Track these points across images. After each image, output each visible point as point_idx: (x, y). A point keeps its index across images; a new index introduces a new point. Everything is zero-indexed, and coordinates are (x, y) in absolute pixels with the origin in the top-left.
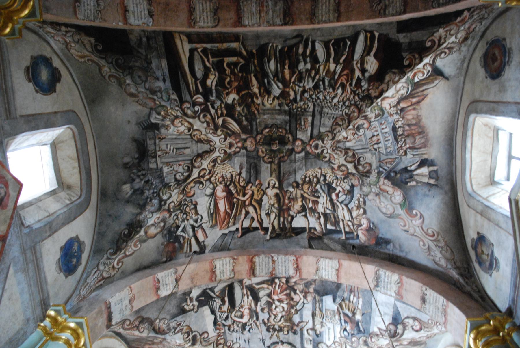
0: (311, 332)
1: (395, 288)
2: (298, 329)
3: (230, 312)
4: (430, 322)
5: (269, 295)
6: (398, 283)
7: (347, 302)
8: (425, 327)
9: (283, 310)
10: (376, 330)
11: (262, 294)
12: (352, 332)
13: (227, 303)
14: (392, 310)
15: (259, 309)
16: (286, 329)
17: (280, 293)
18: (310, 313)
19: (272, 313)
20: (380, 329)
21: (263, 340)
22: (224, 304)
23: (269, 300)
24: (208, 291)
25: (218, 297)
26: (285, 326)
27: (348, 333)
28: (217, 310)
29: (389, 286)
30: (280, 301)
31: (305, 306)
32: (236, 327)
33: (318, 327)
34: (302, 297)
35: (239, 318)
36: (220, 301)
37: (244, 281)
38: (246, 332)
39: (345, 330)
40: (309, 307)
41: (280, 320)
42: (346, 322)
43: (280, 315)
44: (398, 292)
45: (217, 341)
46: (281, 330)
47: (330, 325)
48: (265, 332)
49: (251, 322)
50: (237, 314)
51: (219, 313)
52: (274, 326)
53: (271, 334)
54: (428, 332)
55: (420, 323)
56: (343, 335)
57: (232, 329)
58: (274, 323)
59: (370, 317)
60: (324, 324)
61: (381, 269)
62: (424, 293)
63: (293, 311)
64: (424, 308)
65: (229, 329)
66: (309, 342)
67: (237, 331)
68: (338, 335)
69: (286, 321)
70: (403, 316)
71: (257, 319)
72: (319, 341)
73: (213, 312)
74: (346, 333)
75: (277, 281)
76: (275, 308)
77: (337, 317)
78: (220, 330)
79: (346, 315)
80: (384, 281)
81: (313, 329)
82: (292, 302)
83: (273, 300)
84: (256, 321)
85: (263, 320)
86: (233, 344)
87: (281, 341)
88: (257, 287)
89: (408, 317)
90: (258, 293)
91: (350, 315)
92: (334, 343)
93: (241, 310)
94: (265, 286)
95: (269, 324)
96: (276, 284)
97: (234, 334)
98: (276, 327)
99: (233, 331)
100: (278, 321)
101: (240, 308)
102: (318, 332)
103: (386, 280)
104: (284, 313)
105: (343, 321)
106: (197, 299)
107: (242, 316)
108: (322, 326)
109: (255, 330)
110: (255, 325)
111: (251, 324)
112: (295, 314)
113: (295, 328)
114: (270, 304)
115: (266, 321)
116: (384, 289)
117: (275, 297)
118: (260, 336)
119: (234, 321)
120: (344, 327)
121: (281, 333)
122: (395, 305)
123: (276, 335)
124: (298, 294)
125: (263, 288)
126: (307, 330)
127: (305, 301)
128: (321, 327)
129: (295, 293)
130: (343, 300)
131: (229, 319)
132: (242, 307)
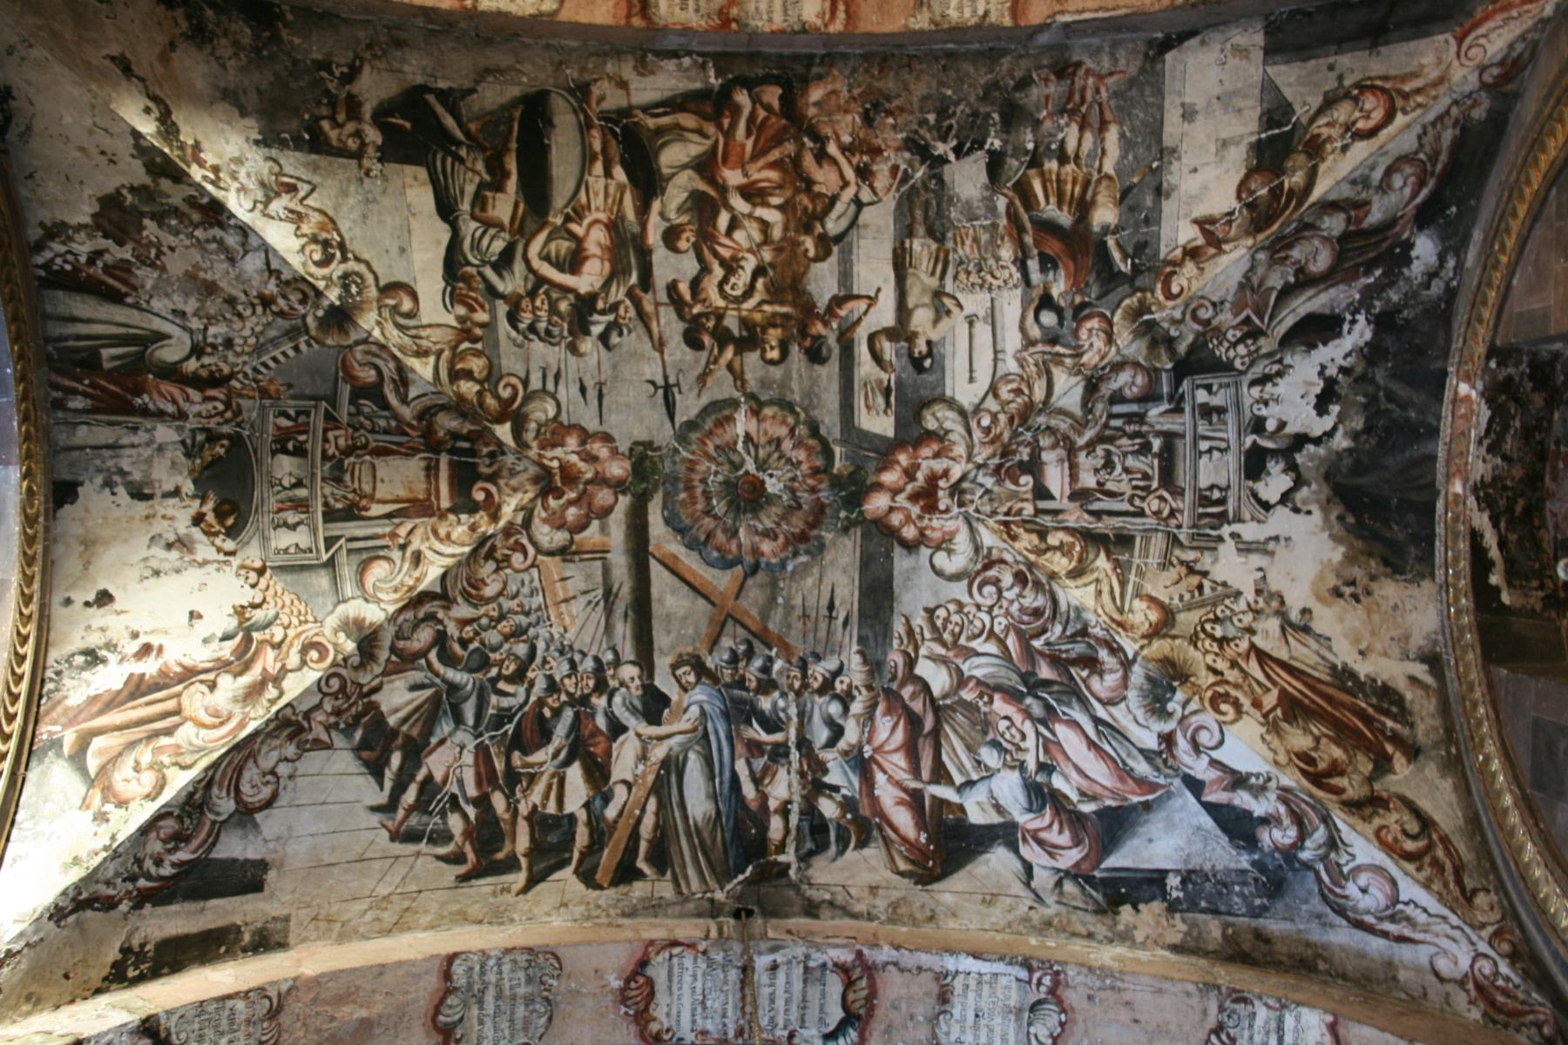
0: (888, 349)
2: (832, 340)
3: (521, 231)
5: (705, 166)
7: (1052, 165)
9: (767, 240)
11: (672, 156)
12: (1078, 299)
13: (512, 184)
15: (654, 237)
16: (774, 335)
17: (755, 157)
18: (886, 250)
19: (716, 254)
21: (667, 388)
22: (498, 187)
23: (702, 186)
24: (431, 98)
25: (474, 142)
26: (771, 322)
27: (1059, 312)
28: (465, 206)
30: (752, 193)
31: (867, 215)
32: (543, 314)
33: (921, 319)
34: (850, 174)
35: (560, 267)
36: (480, 166)
37: (596, 91)
38: (587, 345)
39: (1046, 302)
40: (880, 218)
41: (750, 291)
42: (1047, 263)
43: (750, 264)
45: (456, 356)
46: (750, 339)
47: (975, 303)
48: (677, 350)
49: (618, 293)
50: (553, 246)
51: (474, 225)
52: (720, 317)
53: (704, 355)
56: (1035, 332)
57: (527, 318)
58: (721, 303)
60: (948, 302)
63: (809, 244)
65: (513, 319)
66: (880, 401)
67: (548, 332)
68: (1012, 341)
69: (775, 294)
71: (646, 282)
72: (925, 393)
73: (446, 209)
74: (1048, 318)
75: (742, 98)
76: (729, 232)
77: (1007, 253)
78: (472, 309)
79: (1047, 228)
81: (900, 331)
82: (805, 200)
83: (723, 189)
84: (638, 292)
85: (672, 287)
86: (529, 398)
87: (752, 397)
88: (651, 123)
90: (657, 154)
91: (1065, 218)
92: (993, 390)
93: (574, 227)
94: (688, 120)
95: (696, 310)
96: (736, 110)
97: (537, 346)
98: (731, 322)
99: (532, 328)
100: (738, 292)
101: (568, 219)
102: (921, 346)
104: (767, 255)
105: (1033, 265)
106: (379, 118)
107: (574, 263)
108: (941, 313)
109: (632, 341)
110: (632, 313)
111: (614, 308)
112: (818, 259)
113: (819, 328)
114: (704, 207)
115: (684, 288)
117: (733, 177)
118: (653, 370)
119: (541, 280)
120: (1036, 294)
121: (752, 358)
122: (1269, 87)
123: (730, 367)
124: (834, 161)
125: (678, 132)
126: (872, 338)
127: (866, 195)
128: (936, 321)
129: (821, 156)
130: (1035, 162)
131: (519, 266)
132: (578, 214)
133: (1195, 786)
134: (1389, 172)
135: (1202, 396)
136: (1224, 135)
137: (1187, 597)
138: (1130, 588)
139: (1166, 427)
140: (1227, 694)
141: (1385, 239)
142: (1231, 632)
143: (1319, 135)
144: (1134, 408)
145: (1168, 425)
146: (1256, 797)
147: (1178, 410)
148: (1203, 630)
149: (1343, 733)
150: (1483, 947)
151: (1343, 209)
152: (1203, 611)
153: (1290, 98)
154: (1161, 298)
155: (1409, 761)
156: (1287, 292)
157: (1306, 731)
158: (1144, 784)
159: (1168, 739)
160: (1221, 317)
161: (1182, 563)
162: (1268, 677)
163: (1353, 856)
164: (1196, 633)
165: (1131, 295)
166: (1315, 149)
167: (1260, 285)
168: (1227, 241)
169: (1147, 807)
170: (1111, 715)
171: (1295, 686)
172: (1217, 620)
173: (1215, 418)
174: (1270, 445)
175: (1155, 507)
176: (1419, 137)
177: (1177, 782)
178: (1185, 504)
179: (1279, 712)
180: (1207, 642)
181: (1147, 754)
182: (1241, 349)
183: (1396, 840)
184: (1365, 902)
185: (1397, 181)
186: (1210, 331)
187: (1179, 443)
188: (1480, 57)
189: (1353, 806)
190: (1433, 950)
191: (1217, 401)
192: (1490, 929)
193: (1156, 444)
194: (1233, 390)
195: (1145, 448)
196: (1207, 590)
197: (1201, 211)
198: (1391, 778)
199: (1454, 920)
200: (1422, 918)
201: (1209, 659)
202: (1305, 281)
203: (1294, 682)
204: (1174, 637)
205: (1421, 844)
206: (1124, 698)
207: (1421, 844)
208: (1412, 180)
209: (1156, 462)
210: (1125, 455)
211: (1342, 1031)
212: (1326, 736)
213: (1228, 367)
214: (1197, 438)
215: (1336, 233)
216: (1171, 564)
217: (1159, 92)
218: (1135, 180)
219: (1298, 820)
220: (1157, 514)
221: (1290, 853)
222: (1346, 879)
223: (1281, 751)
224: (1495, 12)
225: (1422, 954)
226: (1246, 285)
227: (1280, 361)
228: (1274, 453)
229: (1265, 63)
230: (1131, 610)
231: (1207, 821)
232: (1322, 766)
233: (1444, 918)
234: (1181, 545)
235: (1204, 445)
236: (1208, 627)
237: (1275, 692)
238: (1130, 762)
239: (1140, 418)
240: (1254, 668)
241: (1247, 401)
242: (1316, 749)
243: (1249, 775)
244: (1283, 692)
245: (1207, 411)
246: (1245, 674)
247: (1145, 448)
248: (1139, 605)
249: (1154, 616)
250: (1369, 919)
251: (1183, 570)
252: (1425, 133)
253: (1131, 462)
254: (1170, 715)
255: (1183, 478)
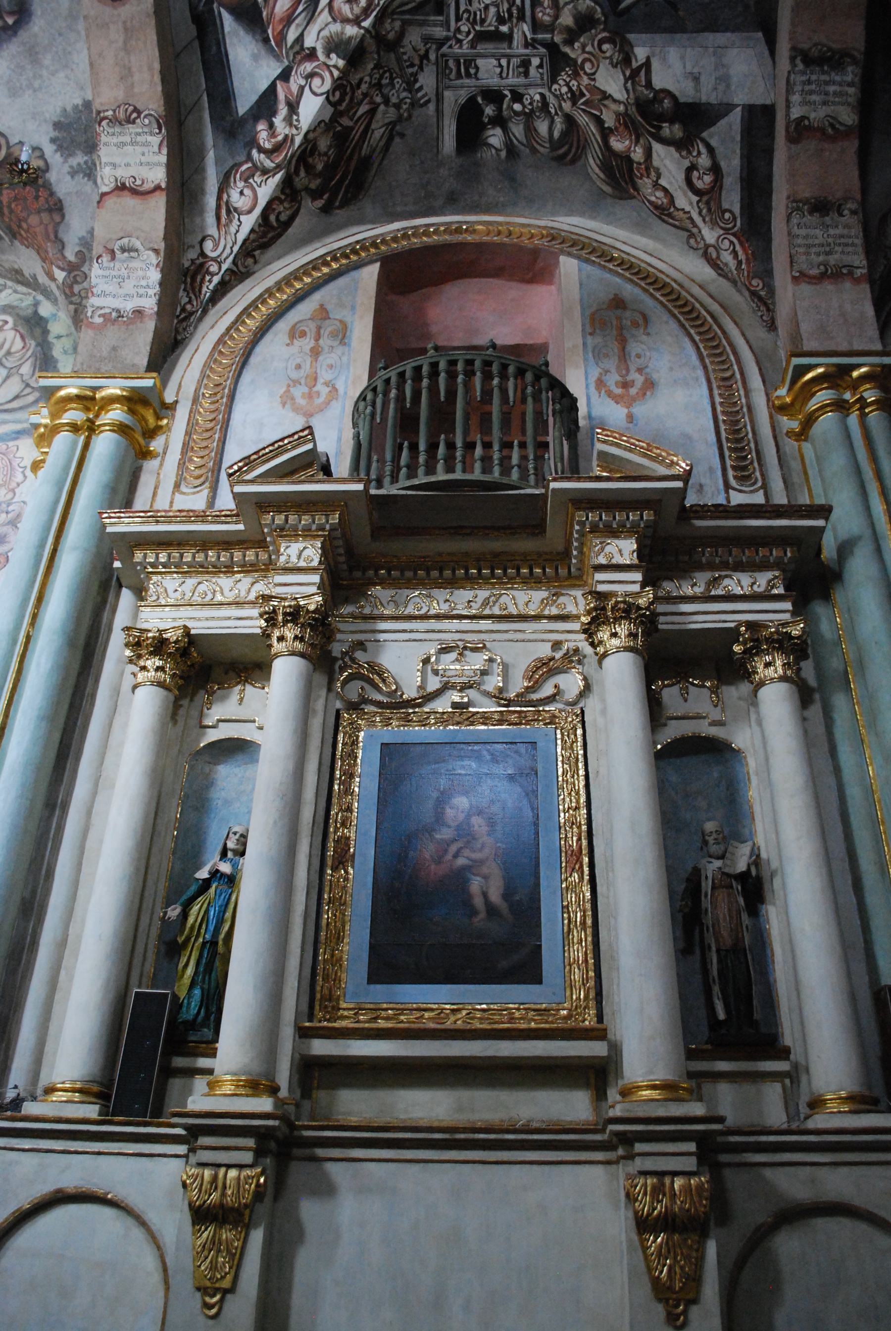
1: (817, 115)
4: (727, 215)
6: (832, 126)
8: (708, 203)
10: (641, 53)
14: (713, 100)
20: (647, 64)
29: (814, 97)
44: (809, 128)
54: (700, 213)
55: (713, 188)
59: (671, 30)
61: (858, 71)
62: (840, 205)
64: (798, 209)
70: (711, 136)
80: (827, 83)
89: (711, 150)
103: (832, 89)
116: (803, 83)
133: (285, 76)
134: (665, 190)
135: (535, 61)
136: (703, 79)
137: (405, 57)
138: (407, 17)
139: (515, 36)
140: (346, 94)
141: (626, 183)
142: (386, 91)
143: (693, 146)
144: (528, 13)
145: (517, 38)
146: (284, 120)
147: (527, 45)
148: (385, 72)
149: (331, 168)
150: (224, 267)
151: (646, 161)
152: (397, 70)
153: (719, 124)
154: (600, 36)
155: (320, 209)
156: (599, 121)
157: (330, 147)
158: (281, 37)
159: (312, 55)
160: (585, 78)
161: (427, 51)
162: (360, 118)
163: (260, 186)
164: (382, 67)
165: (603, 14)
166: (682, 145)
167: (605, 106)
168: (633, 84)
169: (266, 40)
170: (322, 10)
171: (356, 135)
172: (392, 79)
173: (521, 70)
174: (505, 106)
175: (464, 29)
176: (683, 210)
177: (286, 63)
178: (465, 49)
179: (339, 128)
180: (377, 76)
181: (300, 39)
182: (564, 89)
183: (274, 210)
184: (234, 195)
185: (660, 194)
186: (577, 70)
187: (505, 45)
188: (723, 247)
189: (287, 184)
190: (216, 236)
191: (533, 71)
192: (235, 269)
193: (504, 29)
194: (539, 82)
195: (501, 20)
196: (410, 70)
197: (655, 65)
198: (309, 201)
199: (236, 249)
200: (233, 229)
201: (367, 79)
202: (606, 133)
203: (358, 134)
204: (378, 53)
205: (275, 224)
206: (335, 20)
207: (275, 224)
208: (660, 202)
209: (493, 28)
210: (497, 6)
211: (157, 193)
212: (329, 158)
213: (554, 80)
214: (509, 57)
215: (632, 155)
216: (426, 44)
217: (736, 29)
218: (681, 13)
219: (277, 148)
220: (458, 30)
221: (253, 142)
222: (246, 181)
223: (316, 134)
224: (747, 254)
225: (212, 230)
226: (605, 96)
227: (556, 114)
228: (500, 109)
229: (744, 106)
230: (393, 20)
231: (264, 85)
232: (310, 160)
233: (235, 243)
234: (438, 49)
235: (504, 62)
236: (387, 75)
237: (351, 124)
238: (293, 27)
239: (522, 18)
240: (363, 109)
241: (532, 91)
242: (320, 155)
243: (298, 115)
244: (352, 128)
245: (525, 64)
246: (360, 104)
247: (501, 20)
248: (397, 24)
249: (391, 36)
250: (225, 197)
251: (422, 52)
252: (686, 213)
253: (492, 10)
254: (328, 56)
255: (481, 48)
